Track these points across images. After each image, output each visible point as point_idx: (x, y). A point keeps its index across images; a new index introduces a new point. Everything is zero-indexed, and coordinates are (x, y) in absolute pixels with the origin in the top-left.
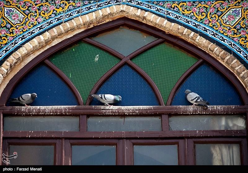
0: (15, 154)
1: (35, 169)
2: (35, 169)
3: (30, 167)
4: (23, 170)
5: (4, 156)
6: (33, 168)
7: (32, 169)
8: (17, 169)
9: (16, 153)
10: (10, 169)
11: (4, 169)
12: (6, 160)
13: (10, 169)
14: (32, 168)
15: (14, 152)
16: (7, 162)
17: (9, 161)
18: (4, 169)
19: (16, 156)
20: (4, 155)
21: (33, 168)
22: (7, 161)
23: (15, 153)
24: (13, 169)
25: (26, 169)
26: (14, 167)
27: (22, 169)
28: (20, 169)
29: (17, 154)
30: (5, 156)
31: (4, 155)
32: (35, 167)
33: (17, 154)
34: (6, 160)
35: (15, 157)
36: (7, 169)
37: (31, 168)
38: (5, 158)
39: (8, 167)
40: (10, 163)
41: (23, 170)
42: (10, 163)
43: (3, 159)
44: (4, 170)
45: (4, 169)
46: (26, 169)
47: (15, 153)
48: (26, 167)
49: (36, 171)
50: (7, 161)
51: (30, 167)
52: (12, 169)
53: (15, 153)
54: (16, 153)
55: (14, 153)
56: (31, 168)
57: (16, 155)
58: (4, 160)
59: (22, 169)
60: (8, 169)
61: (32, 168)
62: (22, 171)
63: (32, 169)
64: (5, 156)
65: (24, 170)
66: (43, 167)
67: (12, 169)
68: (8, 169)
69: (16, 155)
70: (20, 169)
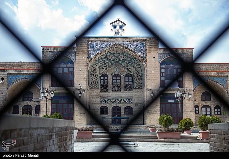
0: (14, 142)
1: (32, 156)
2: (32, 156)
4: (21, 156)
5: (3, 143)
6: (30, 154)
7: (29, 155)
8: (16, 155)
9: (15, 141)
10: (9, 156)
11: (4, 156)
12: (6, 147)
13: (9, 156)
14: (29, 155)
15: (13, 140)
16: (6, 149)
17: (8, 148)
20: (3, 142)
21: (30, 154)
22: (7, 148)
23: (14, 141)
24: (12, 156)
25: (24, 156)
26: (13, 153)
27: (21, 156)
28: (19, 156)
31: (3, 142)
32: (32, 153)
33: (15, 142)
35: (14, 145)
36: (7, 156)
37: (28, 154)
38: (4, 145)
39: (7, 153)
40: (9, 150)
41: (21, 156)
42: (9, 150)
43: (3, 146)
44: (3, 156)
45: (4, 156)
46: (24, 156)
47: (14, 140)
48: (24, 153)
49: (34, 157)
50: (7, 148)
51: (27, 153)
52: (11, 156)
53: (14, 140)
55: (13, 141)
56: (28, 154)
57: (15, 143)
58: (4, 147)
59: (21, 156)
60: (8, 156)
61: (29, 155)
62: (20, 157)
63: (29, 155)
64: (4, 143)
65: (22, 156)
66: (40, 153)
67: (11, 156)
68: (8, 156)
69: (15, 143)
70: (19, 156)
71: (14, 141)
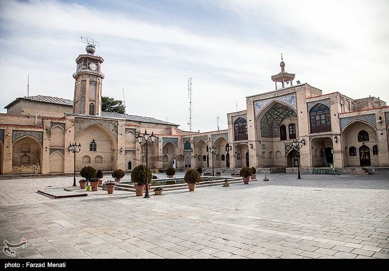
0: (24, 241)
1: (54, 265)
2: (54, 265)
3: (46, 261)
4: (36, 266)
6: (51, 263)
8: (27, 265)
9: (25, 240)
10: (16, 265)
11: (6, 265)
12: (10, 251)
13: (16, 265)
14: (50, 263)
16: (10, 253)
17: (14, 253)
18: (7, 265)
19: (24, 245)
20: (6, 242)
21: (51, 263)
22: (12, 253)
23: (23, 240)
24: (21, 265)
25: (40, 265)
27: (35, 265)
28: (32, 265)
29: (26, 241)
30: (7, 244)
31: (6, 242)
34: (10, 251)
36: (11, 265)
37: (48, 263)
38: (7, 247)
41: (36, 266)
43: (6, 249)
44: (6, 267)
45: (7, 265)
46: (40, 265)
47: (24, 239)
50: (12, 253)
52: (18, 265)
53: (24, 239)
54: (25, 240)
55: (22, 241)
56: (48, 263)
58: (6, 251)
59: (35, 265)
60: (13, 265)
61: (50, 263)
62: (34, 268)
64: (7, 244)
65: (38, 266)
67: (18, 265)
68: (13, 265)
69: (25, 243)
70: (32, 265)
71: (23, 240)
